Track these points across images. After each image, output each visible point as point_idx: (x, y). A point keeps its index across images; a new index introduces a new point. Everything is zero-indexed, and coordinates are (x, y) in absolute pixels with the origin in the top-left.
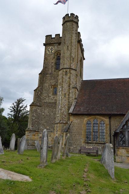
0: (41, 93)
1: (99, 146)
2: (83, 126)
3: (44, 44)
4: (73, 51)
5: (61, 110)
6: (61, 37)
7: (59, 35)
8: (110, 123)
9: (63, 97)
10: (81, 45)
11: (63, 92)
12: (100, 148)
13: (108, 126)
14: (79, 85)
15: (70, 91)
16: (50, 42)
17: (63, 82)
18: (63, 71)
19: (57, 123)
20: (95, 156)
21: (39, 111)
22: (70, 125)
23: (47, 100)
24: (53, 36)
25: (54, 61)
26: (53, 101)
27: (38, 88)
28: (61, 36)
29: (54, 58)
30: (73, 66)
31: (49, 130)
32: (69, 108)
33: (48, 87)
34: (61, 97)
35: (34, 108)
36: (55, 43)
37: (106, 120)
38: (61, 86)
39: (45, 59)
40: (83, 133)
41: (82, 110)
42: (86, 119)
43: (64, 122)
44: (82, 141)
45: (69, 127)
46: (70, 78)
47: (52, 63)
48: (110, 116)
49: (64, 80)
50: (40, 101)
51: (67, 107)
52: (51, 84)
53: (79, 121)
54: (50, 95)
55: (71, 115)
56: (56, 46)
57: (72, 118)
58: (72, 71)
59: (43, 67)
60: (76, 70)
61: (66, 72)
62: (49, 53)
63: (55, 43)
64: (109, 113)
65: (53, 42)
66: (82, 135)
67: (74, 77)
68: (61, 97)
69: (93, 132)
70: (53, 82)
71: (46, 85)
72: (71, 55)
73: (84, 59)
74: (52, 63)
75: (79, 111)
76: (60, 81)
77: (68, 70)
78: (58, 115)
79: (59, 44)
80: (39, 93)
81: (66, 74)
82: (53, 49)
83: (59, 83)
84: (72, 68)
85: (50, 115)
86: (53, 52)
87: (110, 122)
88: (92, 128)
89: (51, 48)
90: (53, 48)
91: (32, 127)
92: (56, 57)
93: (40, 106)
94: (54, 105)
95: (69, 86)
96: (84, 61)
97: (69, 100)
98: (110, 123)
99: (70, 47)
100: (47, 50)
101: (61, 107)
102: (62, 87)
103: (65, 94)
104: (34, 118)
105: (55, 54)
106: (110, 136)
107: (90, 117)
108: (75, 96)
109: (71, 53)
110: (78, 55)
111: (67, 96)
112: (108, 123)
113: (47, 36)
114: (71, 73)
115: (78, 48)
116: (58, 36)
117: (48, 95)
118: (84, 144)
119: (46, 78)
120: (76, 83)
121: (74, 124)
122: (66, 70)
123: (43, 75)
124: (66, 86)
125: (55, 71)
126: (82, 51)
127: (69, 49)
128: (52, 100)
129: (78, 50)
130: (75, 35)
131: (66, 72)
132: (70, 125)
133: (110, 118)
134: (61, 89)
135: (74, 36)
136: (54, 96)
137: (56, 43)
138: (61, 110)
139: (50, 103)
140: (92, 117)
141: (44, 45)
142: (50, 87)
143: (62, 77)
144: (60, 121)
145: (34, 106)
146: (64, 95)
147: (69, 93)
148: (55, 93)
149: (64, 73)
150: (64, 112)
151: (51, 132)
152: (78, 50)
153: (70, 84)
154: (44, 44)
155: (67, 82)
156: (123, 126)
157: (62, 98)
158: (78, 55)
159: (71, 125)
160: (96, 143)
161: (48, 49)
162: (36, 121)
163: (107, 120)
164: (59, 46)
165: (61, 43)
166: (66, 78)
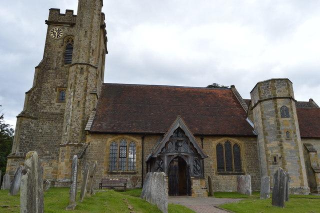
0: (39, 98)
1: (127, 177)
2: (105, 149)
3: (46, 21)
4: (94, 39)
5: (71, 125)
6: (76, 16)
7: (72, 11)
8: (143, 145)
9: (75, 106)
10: (105, 33)
11: (75, 99)
12: (129, 179)
13: (141, 149)
14: (99, 90)
15: (87, 98)
16: (55, 19)
17: (76, 83)
18: (77, 68)
19: (65, 146)
20: (122, 191)
21: (33, 125)
22: (87, 147)
23: (47, 109)
24: (63, 12)
25: (61, 50)
26: (58, 111)
27: (32, 89)
28: (75, 13)
29: (62, 45)
30: (93, 62)
31: (50, 155)
32: (84, 124)
33: (50, 88)
34: (73, 107)
35: (25, 121)
36: (64, 23)
37: (137, 141)
38: (72, 90)
39: (48, 45)
40: (104, 160)
41: (105, 126)
42: (110, 139)
43: (75, 144)
44: (104, 170)
45: (85, 150)
46: (87, 79)
47: (59, 52)
48: (143, 136)
49: (78, 81)
50: (35, 110)
51: (80, 122)
52: (55, 85)
53: (99, 142)
54: (53, 102)
55: (88, 133)
56: (66, 28)
58: (91, 69)
59: (44, 56)
60: (97, 68)
61: (82, 69)
62: (54, 36)
63: (64, 23)
64: (143, 131)
65: (61, 21)
66: (103, 162)
67: (93, 77)
68: (71, 106)
69: (120, 157)
70: (59, 82)
71: (48, 86)
72: (90, 45)
73: (107, 52)
74: (59, 52)
75: (100, 127)
76: (71, 82)
77: (85, 67)
78: (66, 134)
79: (72, 25)
80: (35, 97)
81: (82, 73)
82: (61, 32)
83: (69, 85)
84: (91, 64)
85: (52, 132)
86: (60, 35)
87: (143, 144)
88: (118, 153)
89: (57, 29)
90: (61, 30)
91: (20, 151)
92: (65, 44)
93: (36, 119)
94: (60, 117)
95: (86, 91)
96: (106, 55)
97: (84, 110)
98: (143, 145)
99: (89, 33)
100: (52, 31)
101: (71, 121)
102: (75, 91)
103: (79, 102)
104: (24, 138)
105: (64, 40)
106: (143, 163)
107: (116, 137)
108: (94, 105)
109: (90, 42)
110: (100, 46)
111: (82, 106)
112: (140, 146)
113: (52, 10)
114: (89, 72)
115: (100, 36)
116: (71, 13)
117: (50, 102)
118: (106, 175)
119: (47, 75)
120: (96, 87)
121: (92, 147)
122: (82, 66)
123: (42, 70)
124: (80, 90)
125: (62, 66)
126: (106, 40)
127: (88, 35)
128: (56, 109)
129: (100, 39)
130: (98, 16)
131: (82, 69)
132: (87, 147)
133: (143, 138)
134: (72, 94)
135: (96, 18)
136: (59, 104)
138: (71, 125)
139: (52, 114)
140: (119, 136)
141: (47, 22)
142: (54, 89)
143: (76, 76)
144: (70, 142)
145: (25, 117)
146: (77, 104)
147: (86, 100)
148: (62, 99)
149: (79, 71)
150: (76, 129)
151: (53, 158)
152: (100, 39)
153: (87, 88)
154: (46, 21)
155: (82, 84)
156: (162, 149)
157: (74, 107)
158: (100, 46)
159: (89, 149)
160: (122, 173)
161: (53, 30)
162: (28, 142)
163: (138, 141)
165: (75, 24)
166: (82, 78)
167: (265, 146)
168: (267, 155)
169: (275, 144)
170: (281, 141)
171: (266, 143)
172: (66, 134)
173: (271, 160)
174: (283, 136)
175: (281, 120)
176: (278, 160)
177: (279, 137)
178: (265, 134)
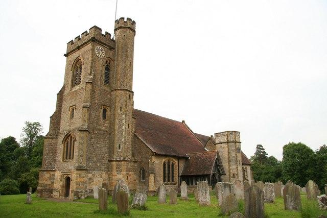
9: (127, 127)
34: (126, 128)
36: (106, 45)
48: (179, 158)
57: (154, 158)
78: (119, 150)
101: (125, 140)
134: (124, 116)
137: (108, 46)
138: (125, 144)
163: (176, 161)
164: (109, 51)
167: (229, 168)
168: (230, 173)
169: (234, 167)
170: (237, 166)
171: (230, 166)
172: (119, 150)
173: (232, 176)
174: (238, 162)
175: (238, 154)
176: (235, 175)
177: (237, 163)
178: (229, 161)
